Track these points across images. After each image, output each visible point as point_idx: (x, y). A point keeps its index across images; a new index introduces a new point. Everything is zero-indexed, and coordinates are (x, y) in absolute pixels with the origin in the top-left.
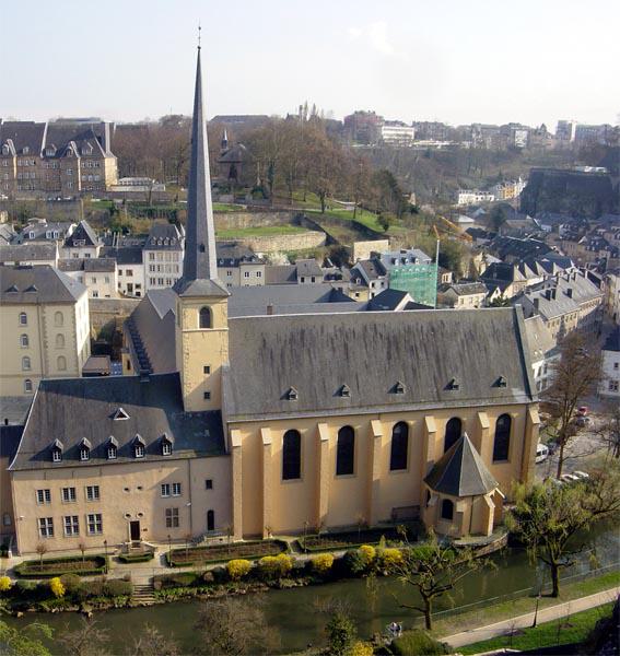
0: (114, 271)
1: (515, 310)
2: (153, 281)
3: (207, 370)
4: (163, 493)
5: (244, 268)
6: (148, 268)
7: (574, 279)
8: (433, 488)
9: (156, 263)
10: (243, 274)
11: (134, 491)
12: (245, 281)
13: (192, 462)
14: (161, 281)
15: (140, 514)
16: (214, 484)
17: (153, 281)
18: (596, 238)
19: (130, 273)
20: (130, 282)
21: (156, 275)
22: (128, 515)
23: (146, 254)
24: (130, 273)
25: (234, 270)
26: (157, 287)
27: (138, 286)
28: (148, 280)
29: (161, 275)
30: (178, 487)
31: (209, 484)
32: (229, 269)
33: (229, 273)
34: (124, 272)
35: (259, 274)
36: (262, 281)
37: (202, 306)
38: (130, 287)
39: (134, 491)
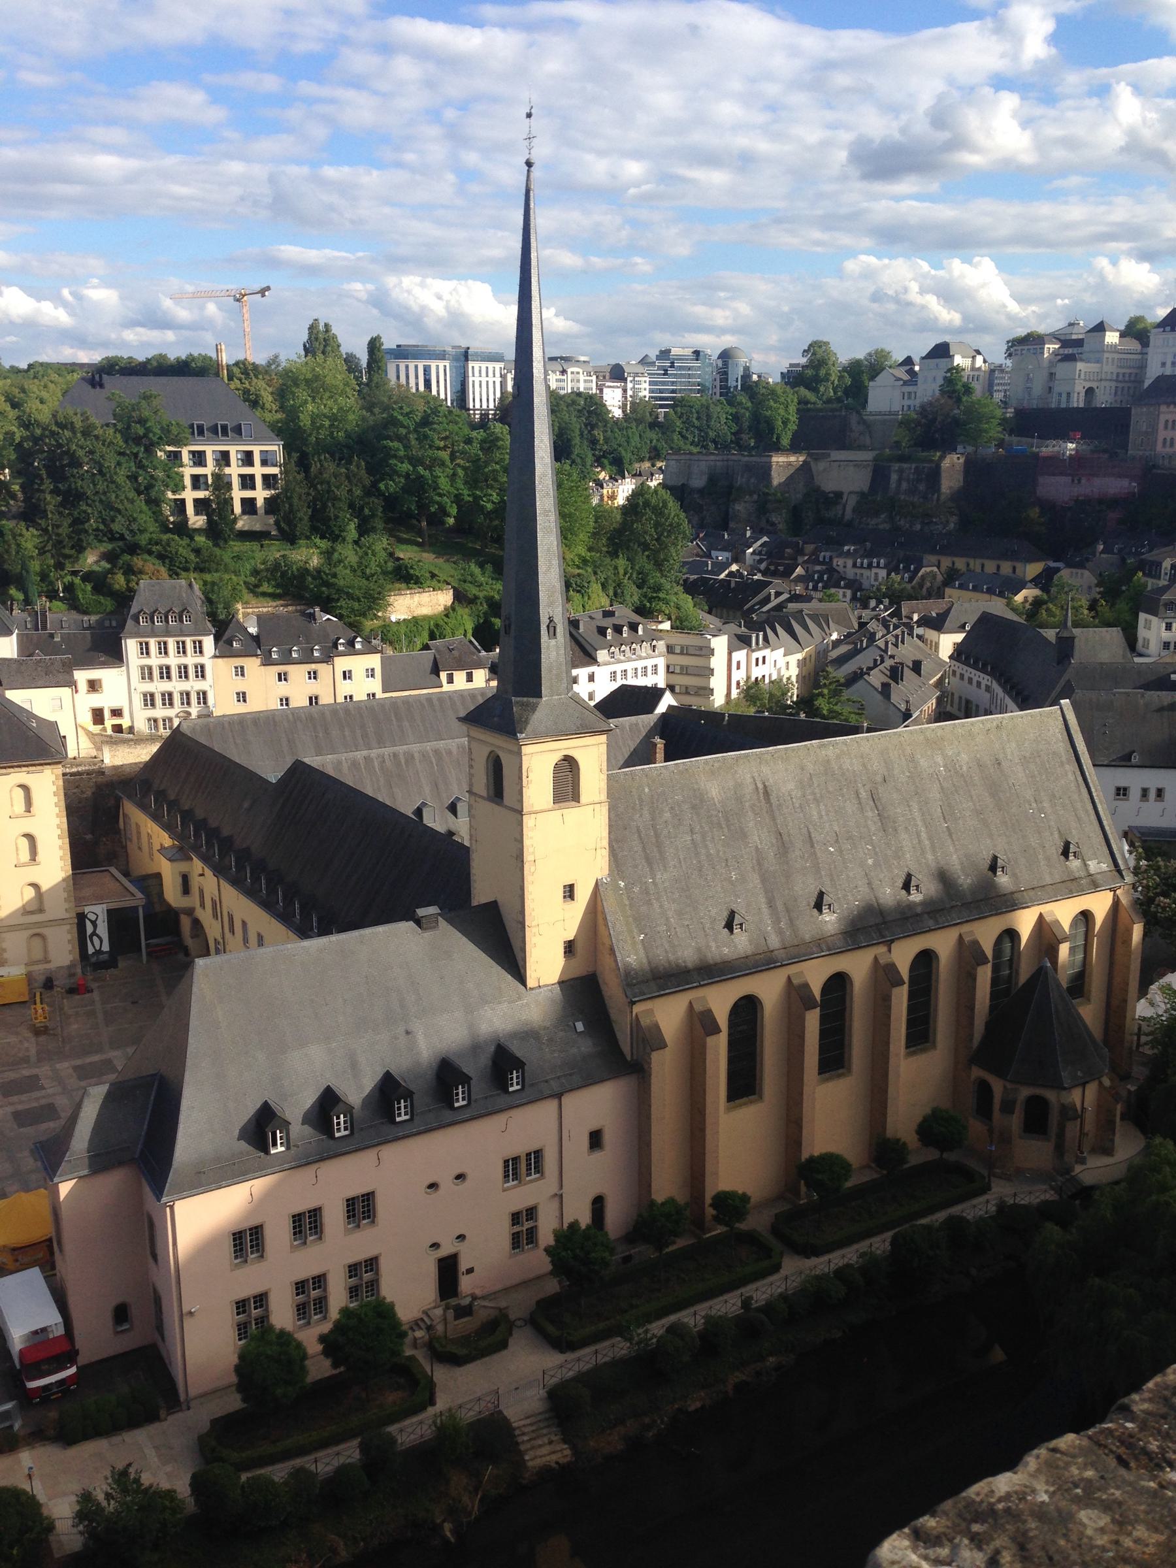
0: (72, 684)
1: (1061, 709)
2: (149, 700)
3: (570, 892)
4: (506, 1176)
5: (342, 663)
6: (135, 674)
7: (903, 642)
8: (1000, 1073)
9: (155, 660)
10: (339, 676)
11: (446, 1182)
12: (345, 688)
13: (567, 1100)
14: (168, 699)
15: (461, 1237)
16: (608, 1138)
17: (149, 700)
18: (818, 568)
19: (94, 686)
20: (97, 705)
21: (158, 686)
22: (435, 1246)
23: (131, 646)
24: (94, 686)
25: (323, 669)
26: (160, 712)
27: (117, 713)
28: (138, 701)
29: (166, 686)
30: (535, 1159)
31: (596, 1140)
32: (313, 666)
33: (313, 675)
34: (83, 686)
35: (371, 673)
36: (375, 686)
37: (557, 757)
38: (98, 716)
39: (446, 1182)
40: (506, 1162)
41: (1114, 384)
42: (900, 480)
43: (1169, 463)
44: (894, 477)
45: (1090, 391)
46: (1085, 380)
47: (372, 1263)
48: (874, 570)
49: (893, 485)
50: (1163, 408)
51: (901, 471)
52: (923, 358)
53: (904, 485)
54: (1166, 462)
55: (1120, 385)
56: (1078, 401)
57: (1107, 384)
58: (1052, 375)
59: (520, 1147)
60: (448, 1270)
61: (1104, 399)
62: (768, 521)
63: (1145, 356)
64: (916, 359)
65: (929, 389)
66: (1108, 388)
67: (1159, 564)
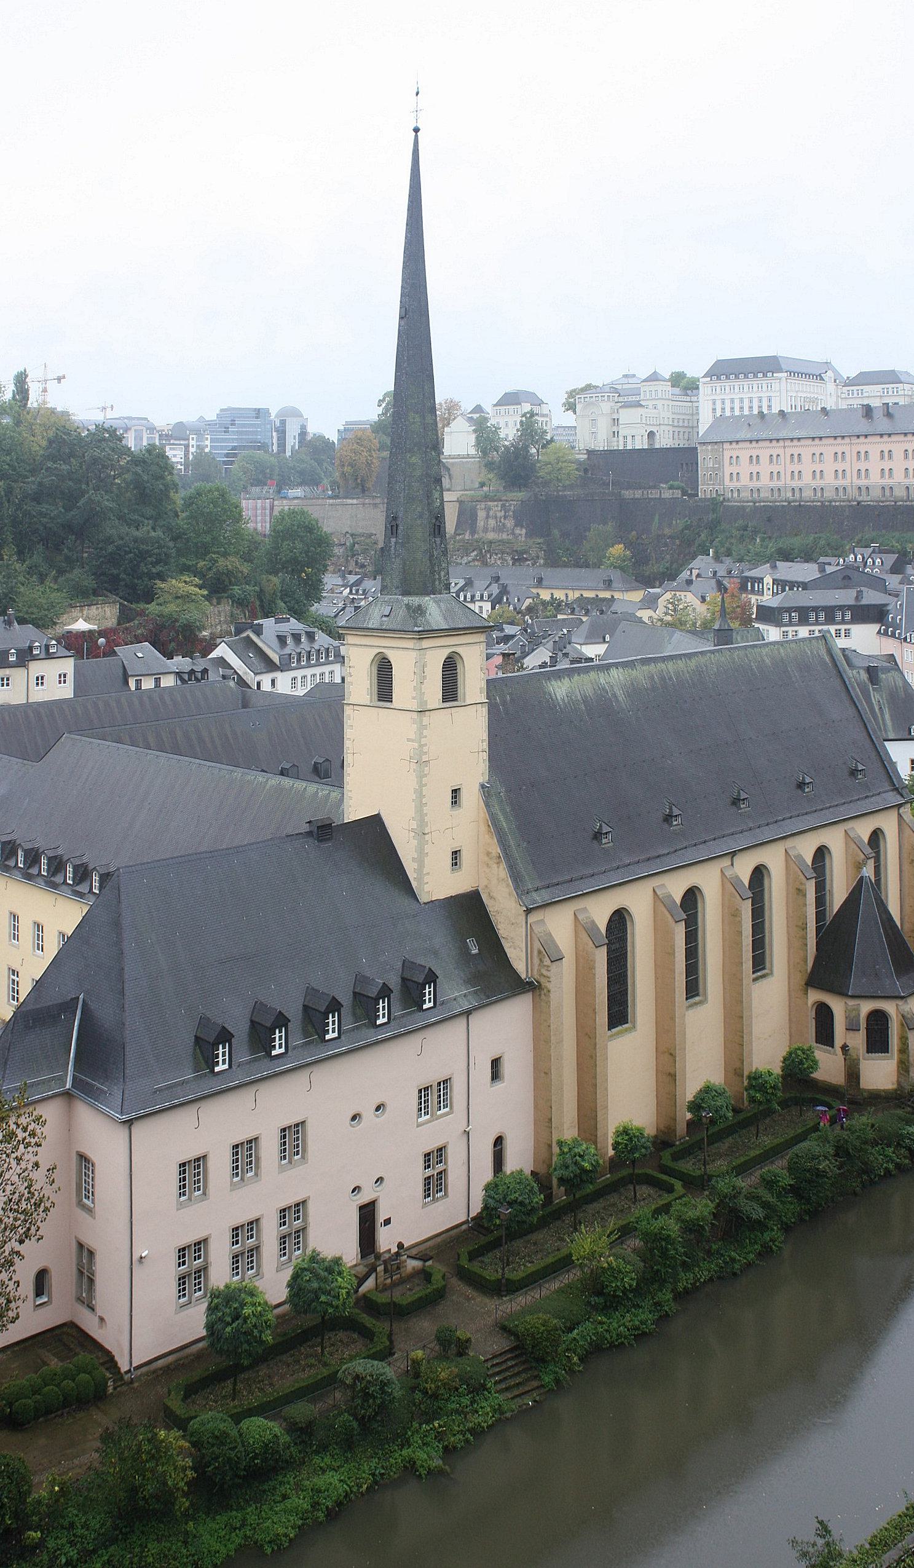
13: (476, 1019)
37: (444, 653)
40: (420, 1091)
41: (671, 429)
42: (488, 517)
43: (739, 496)
44: (481, 514)
45: (651, 435)
46: (647, 425)
47: (300, 1206)
48: (478, 604)
49: (480, 524)
50: (726, 446)
51: (488, 509)
52: (495, 405)
53: (492, 523)
54: (735, 495)
55: (677, 430)
56: (641, 444)
57: (667, 428)
58: (615, 421)
59: (432, 1077)
60: (368, 1215)
61: (664, 441)
62: (357, 563)
63: (695, 404)
64: (488, 408)
65: (509, 430)
66: (666, 432)
67: (760, 580)
